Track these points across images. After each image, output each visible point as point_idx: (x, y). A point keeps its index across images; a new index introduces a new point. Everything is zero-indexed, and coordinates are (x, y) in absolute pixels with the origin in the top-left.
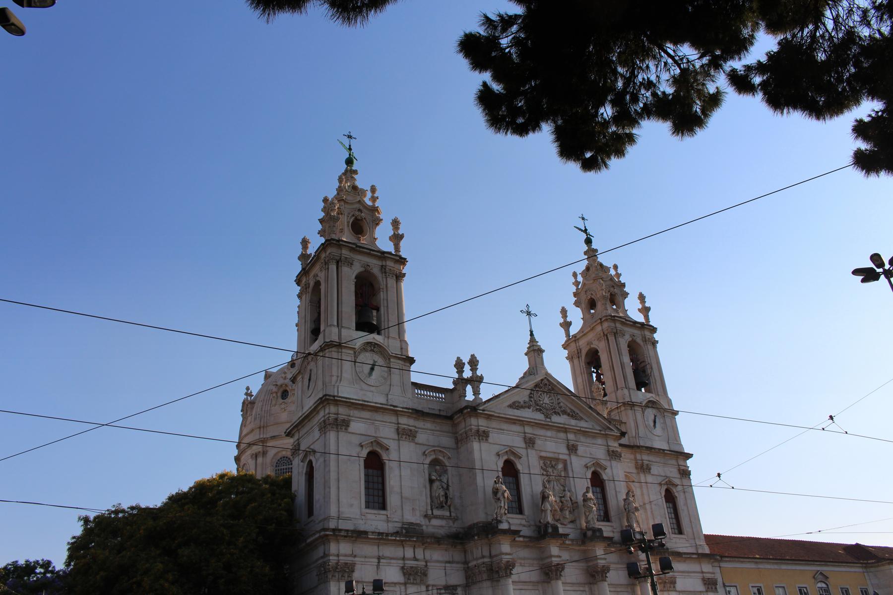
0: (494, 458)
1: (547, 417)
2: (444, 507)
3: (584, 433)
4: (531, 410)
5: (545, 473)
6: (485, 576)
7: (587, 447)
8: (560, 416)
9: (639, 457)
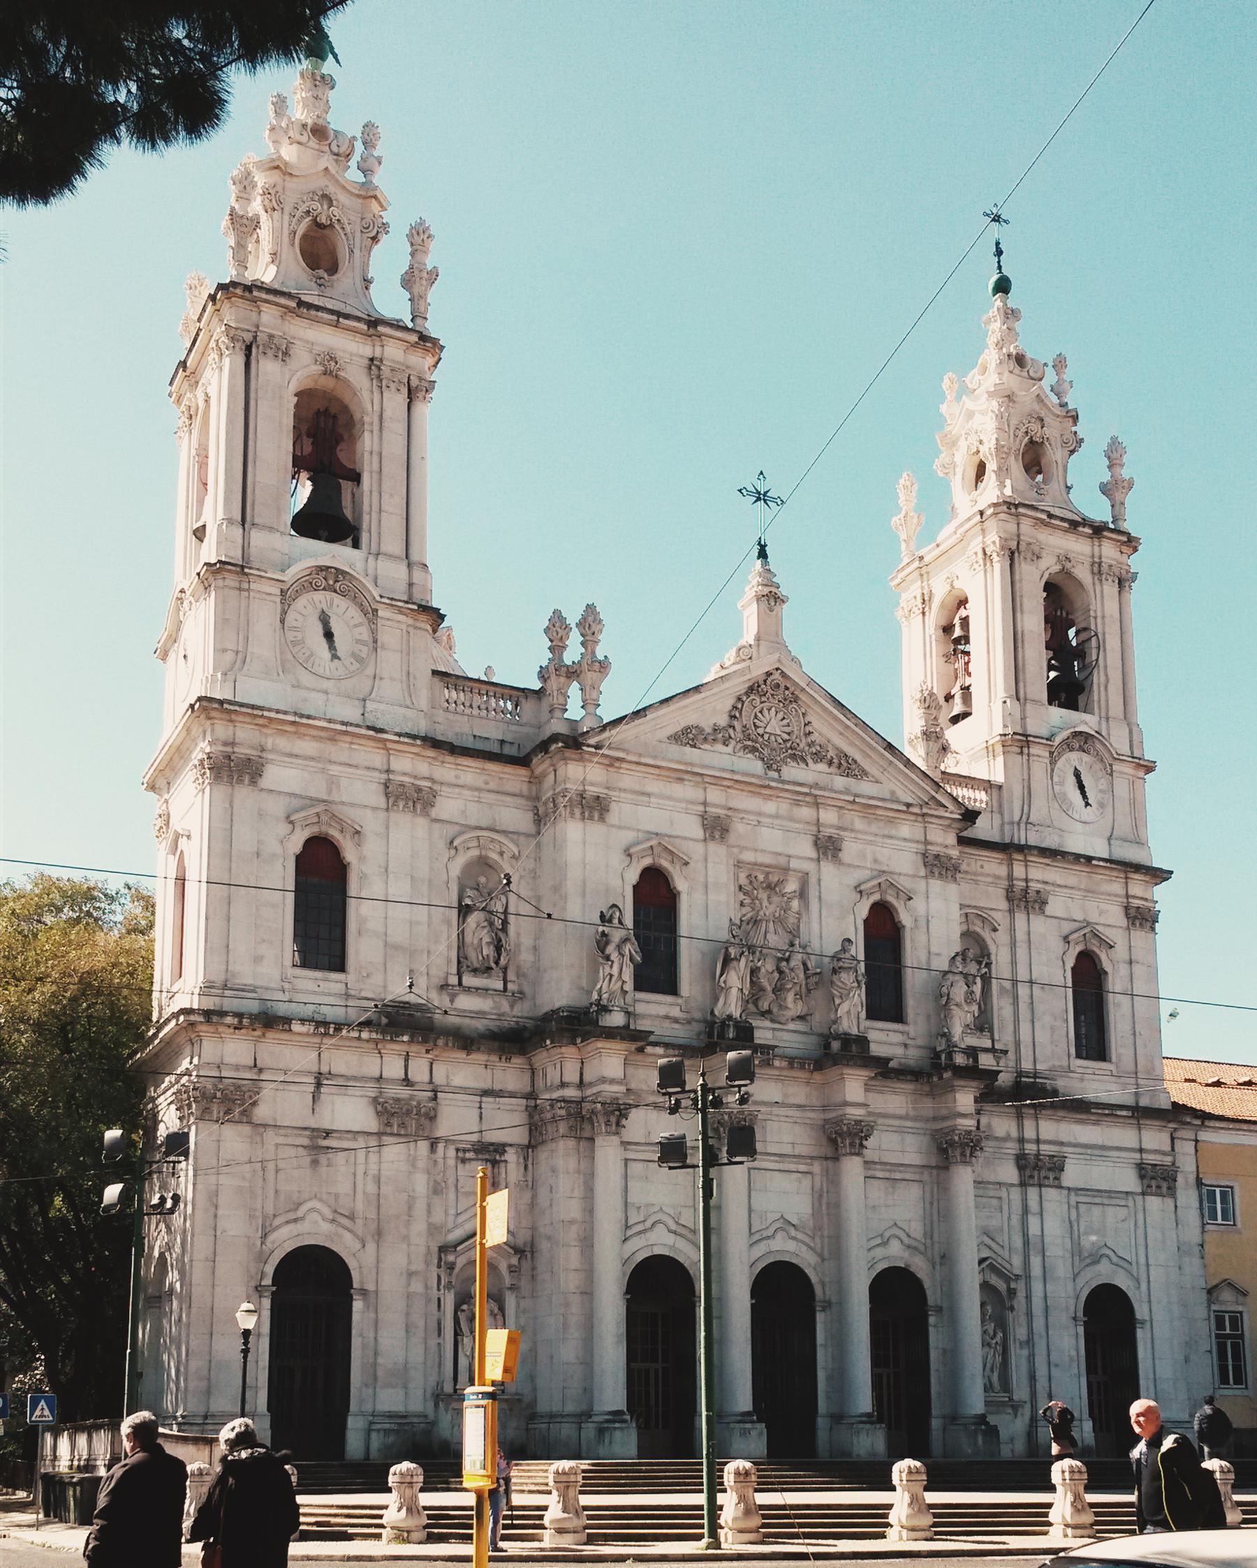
0: (617, 860)
1: (769, 768)
2: (492, 969)
3: (868, 809)
4: (729, 749)
5: (747, 901)
6: (563, 1128)
7: (870, 843)
8: (807, 765)
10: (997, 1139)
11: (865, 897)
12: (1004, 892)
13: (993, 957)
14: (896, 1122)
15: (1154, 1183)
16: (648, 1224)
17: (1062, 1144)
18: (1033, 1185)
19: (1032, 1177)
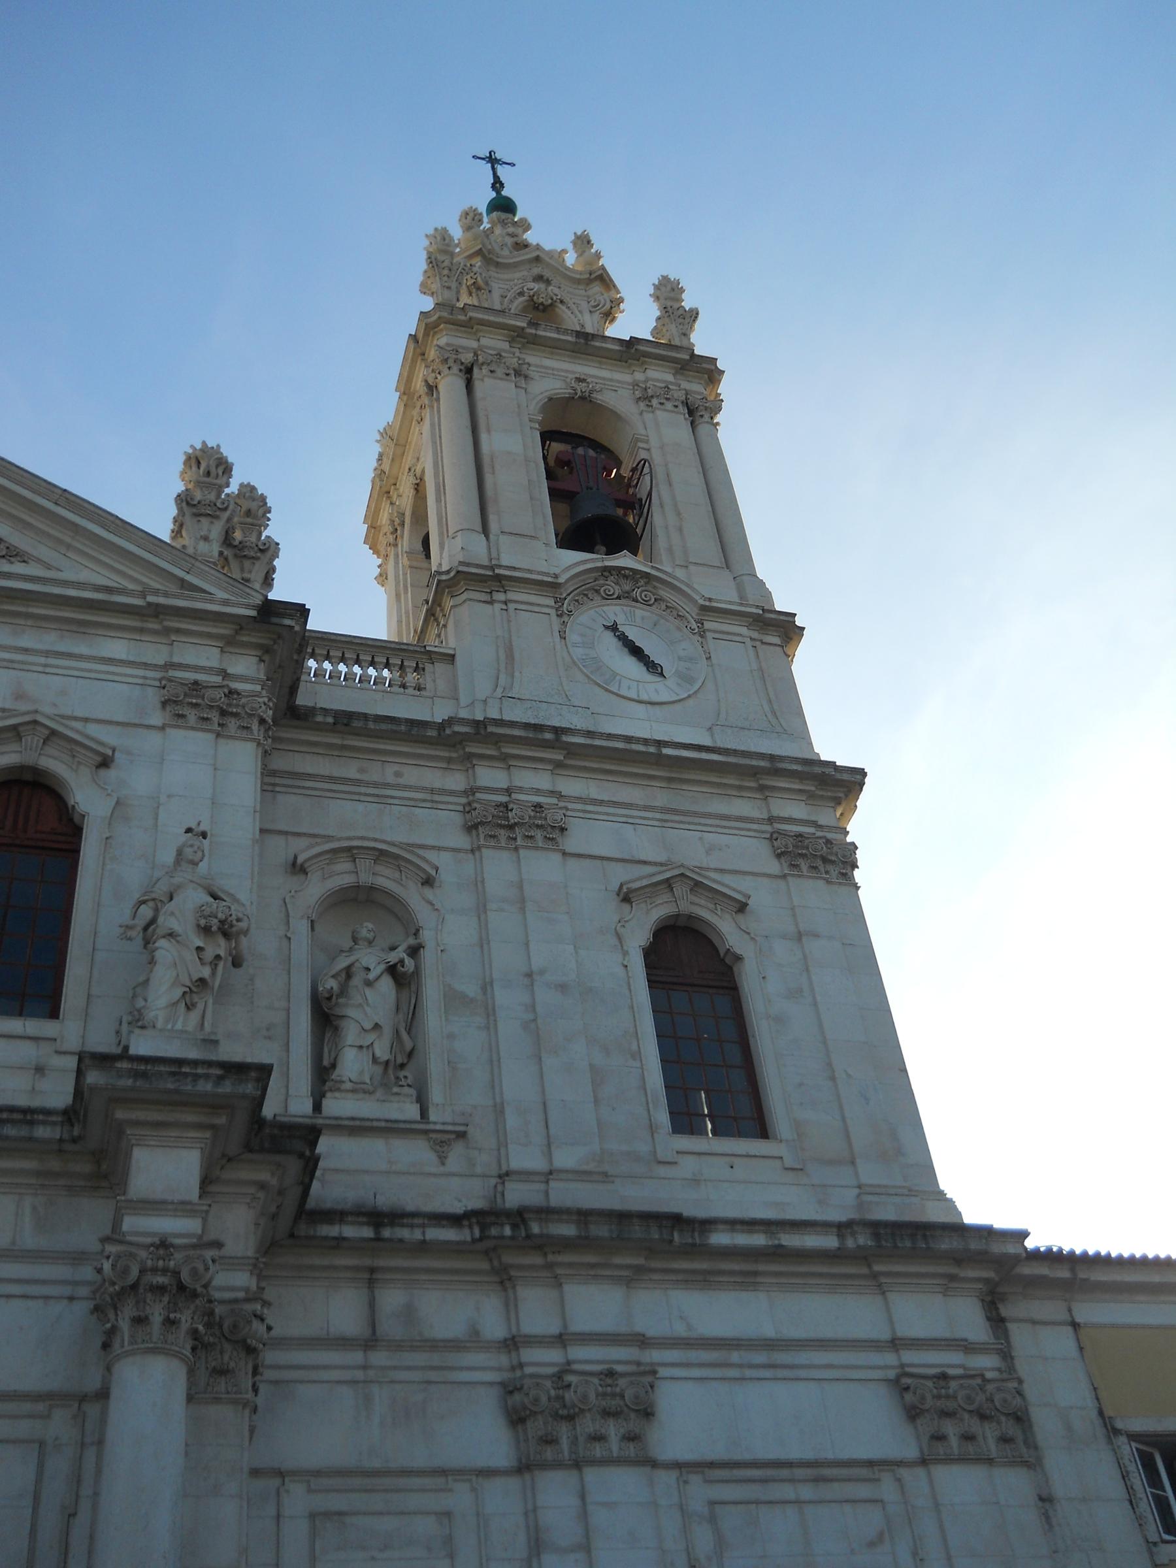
9: (490, 776)
10: (434, 1345)
12: (458, 819)
13: (427, 936)
15: (951, 1429)
17: (642, 1341)
18: (558, 1465)
19: (549, 1440)
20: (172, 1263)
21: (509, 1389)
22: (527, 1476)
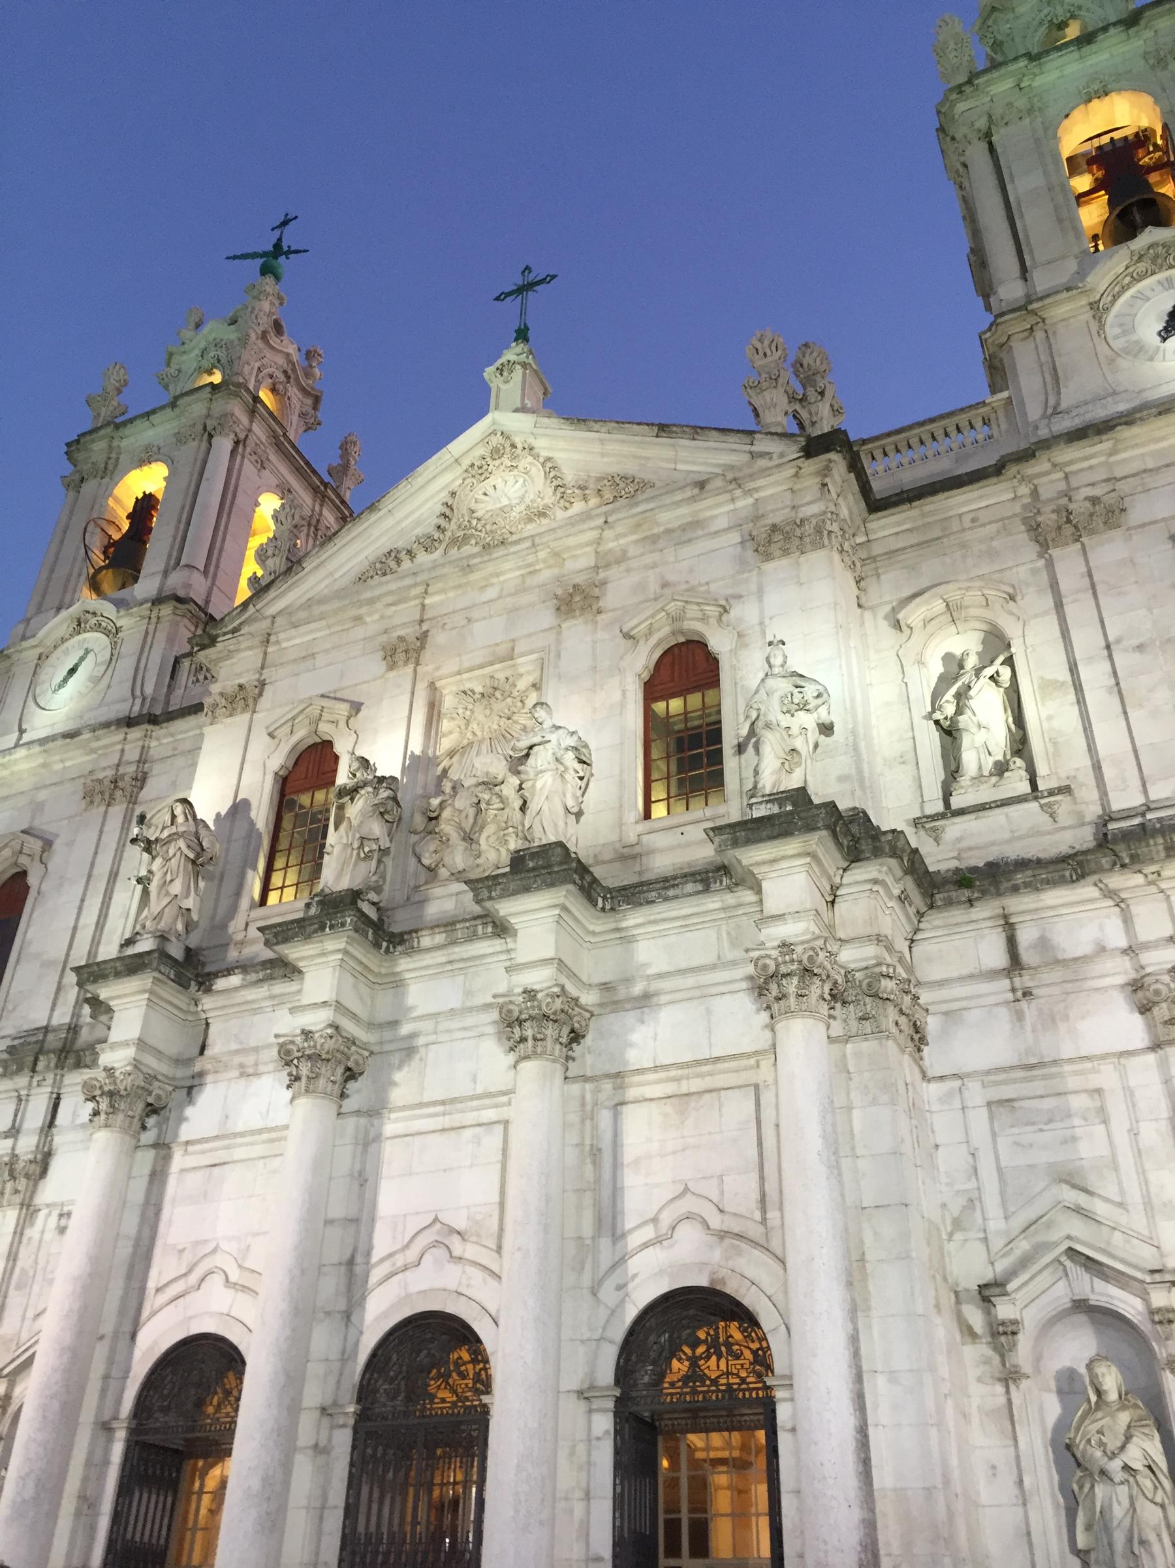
4: (437, 554)
7: (654, 566)
11: (642, 642)
14: (690, 981)
16: (193, 1279)
20: (795, 956)
21: (1136, 986)
22: (1160, 1052)
